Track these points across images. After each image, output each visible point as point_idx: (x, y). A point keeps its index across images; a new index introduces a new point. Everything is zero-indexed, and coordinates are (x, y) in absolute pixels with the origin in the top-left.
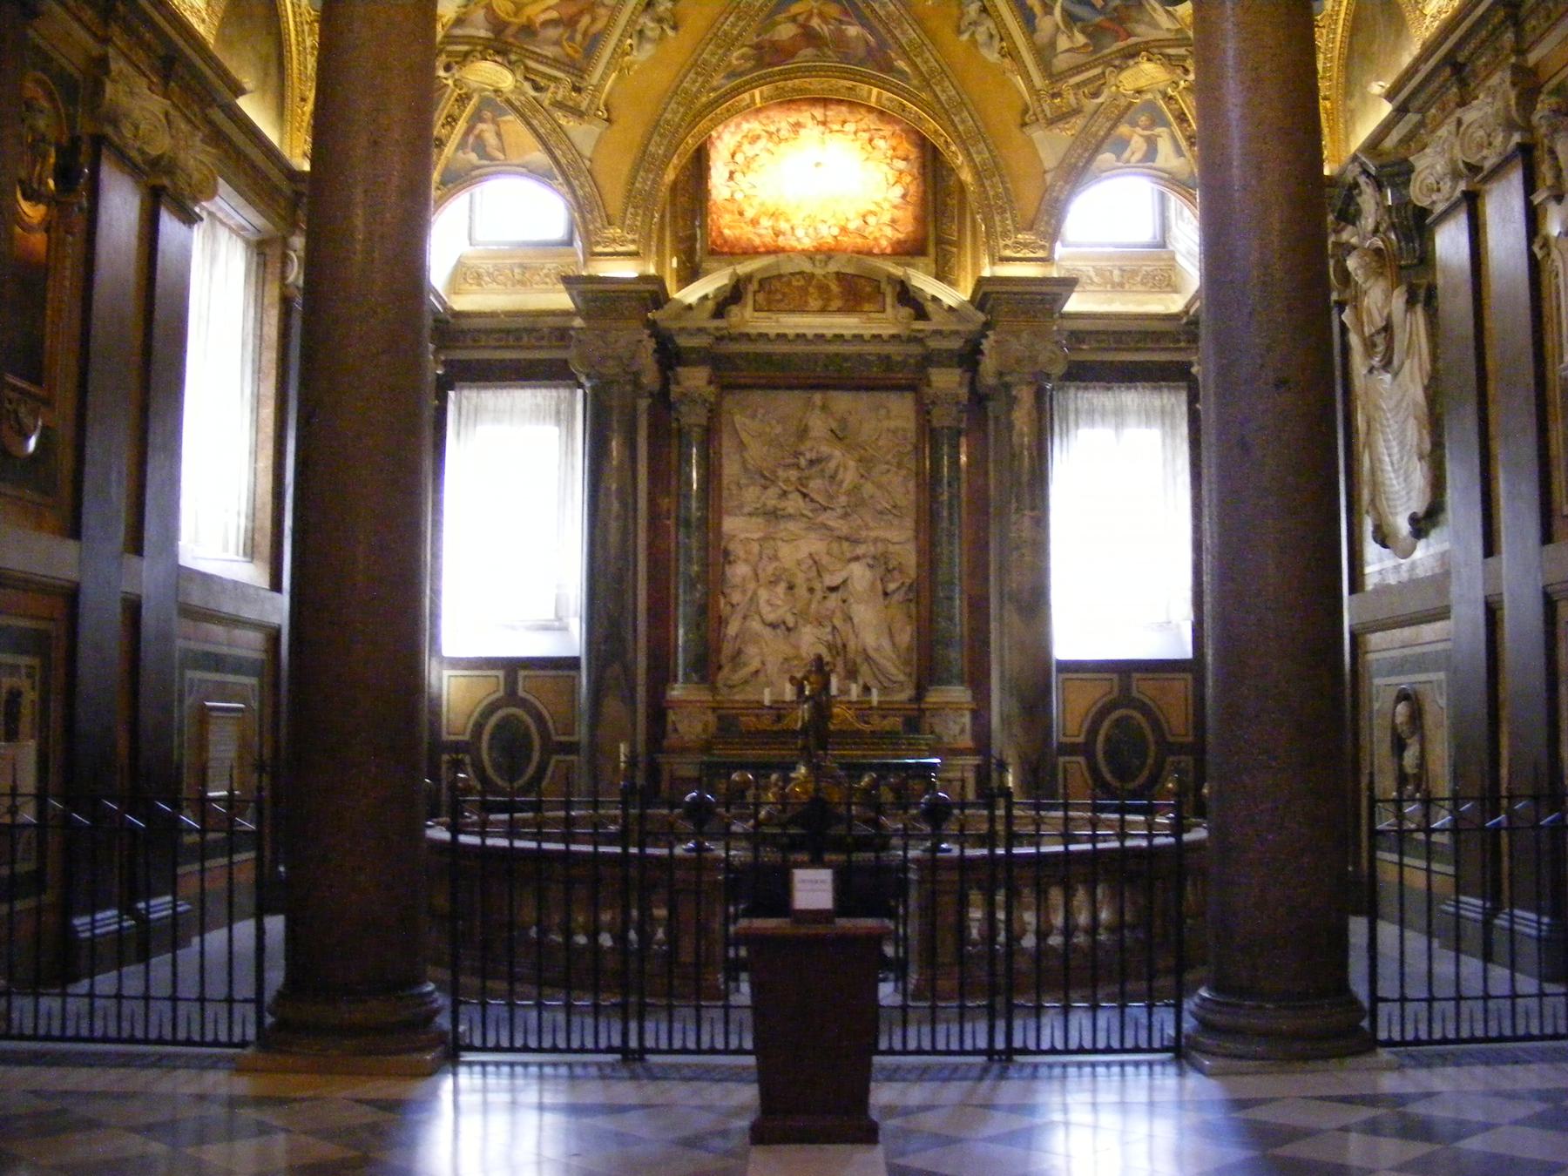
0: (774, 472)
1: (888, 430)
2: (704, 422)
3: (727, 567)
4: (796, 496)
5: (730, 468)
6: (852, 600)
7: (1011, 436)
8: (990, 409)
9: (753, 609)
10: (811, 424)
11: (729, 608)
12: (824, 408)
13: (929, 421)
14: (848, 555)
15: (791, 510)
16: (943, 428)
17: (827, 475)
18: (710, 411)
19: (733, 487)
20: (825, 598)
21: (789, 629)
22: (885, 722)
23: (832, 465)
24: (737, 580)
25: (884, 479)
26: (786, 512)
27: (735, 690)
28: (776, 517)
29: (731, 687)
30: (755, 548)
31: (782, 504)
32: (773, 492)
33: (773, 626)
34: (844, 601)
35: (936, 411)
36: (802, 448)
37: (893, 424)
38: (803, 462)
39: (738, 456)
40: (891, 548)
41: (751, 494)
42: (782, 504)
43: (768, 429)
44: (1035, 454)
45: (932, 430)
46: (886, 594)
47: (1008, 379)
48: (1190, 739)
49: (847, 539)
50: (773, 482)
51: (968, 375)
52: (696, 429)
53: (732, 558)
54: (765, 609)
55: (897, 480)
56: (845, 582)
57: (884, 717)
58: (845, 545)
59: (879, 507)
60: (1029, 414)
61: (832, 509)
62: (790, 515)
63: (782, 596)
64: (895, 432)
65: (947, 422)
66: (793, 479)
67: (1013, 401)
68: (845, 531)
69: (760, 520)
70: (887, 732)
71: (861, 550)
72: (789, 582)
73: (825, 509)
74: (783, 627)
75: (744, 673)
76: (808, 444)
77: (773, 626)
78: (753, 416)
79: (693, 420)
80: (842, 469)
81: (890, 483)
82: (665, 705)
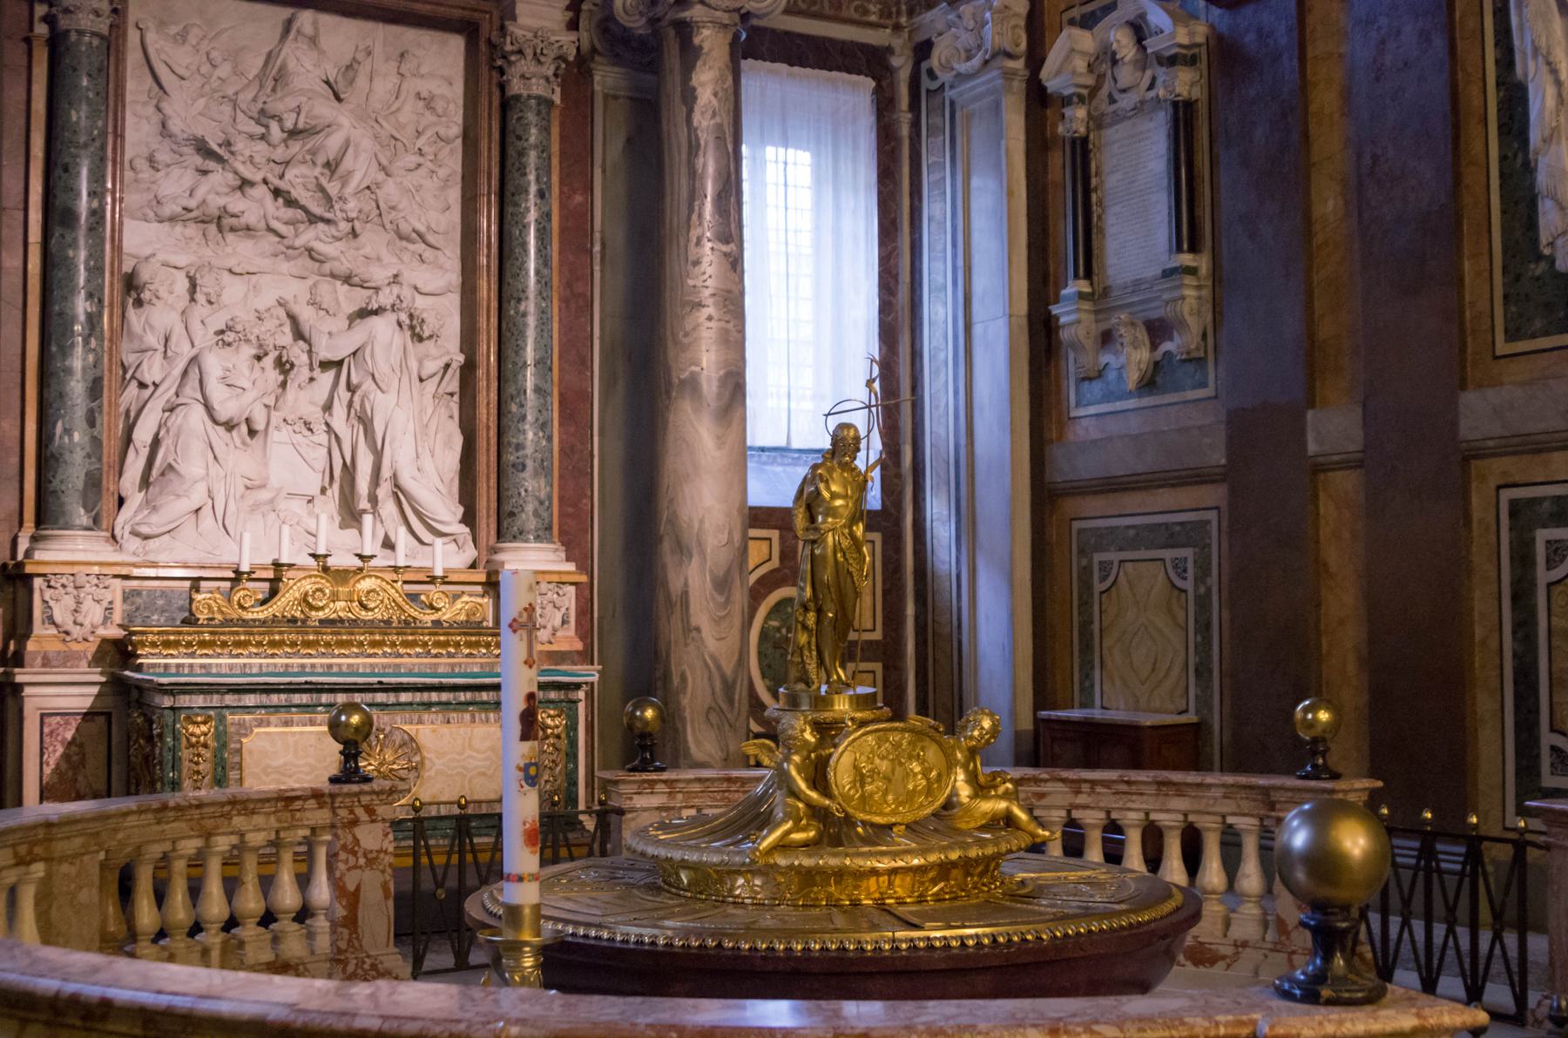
0: (228, 144)
1: (418, 96)
2: (105, 30)
3: (131, 313)
4: (261, 192)
5: (138, 131)
6: (368, 385)
7: (690, 111)
8: (597, 78)
9: (191, 389)
10: (292, 65)
11: (133, 389)
12: (313, 41)
13: (502, 87)
14: (354, 308)
15: (252, 218)
16: (529, 97)
17: (321, 159)
18: (115, 11)
19: (141, 164)
20: (312, 379)
21: (252, 433)
22: (459, 605)
23: (333, 144)
24: (152, 340)
25: (410, 180)
26: (243, 220)
27: (152, 544)
28: (220, 229)
29: (146, 538)
30: (182, 285)
31: (236, 203)
32: (220, 178)
33: (230, 426)
34: (351, 388)
35: (525, 66)
36: (277, 106)
37: (425, 87)
38: (276, 132)
39: (151, 110)
40: (421, 302)
41: (176, 185)
42: (236, 203)
43: (205, 68)
44: (730, 148)
45: (507, 105)
46: (421, 380)
47: (686, 14)
48: (877, 635)
49: (347, 280)
50: (219, 159)
51: (570, 14)
52: (96, 42)
53: (146, 295)
54: (217, 392)
55: (430, 185)
56: (354, 354)
57: (456, 597)
58: (343, 289)
59: (405, 228)
60: (722, 79)
61: (328, 222)
62: (248, 228)
63: (246, 372)
64: (428, 102)
65: (538, 88)
66: (257, 159)
67: (690, 54)
68: (343, 267)
69: (192, 230)
70: (461, 624)
71: (385, 298)
72: (261, 346)
73: (313, 219)
74: (244, 428)
75: (175, 507)
76: (291, 102)
77: (230, 426)
78: (182, 37)
79: (85, 21)
80: (351, 150)
81: (419, 188)
82: (29, 569)
